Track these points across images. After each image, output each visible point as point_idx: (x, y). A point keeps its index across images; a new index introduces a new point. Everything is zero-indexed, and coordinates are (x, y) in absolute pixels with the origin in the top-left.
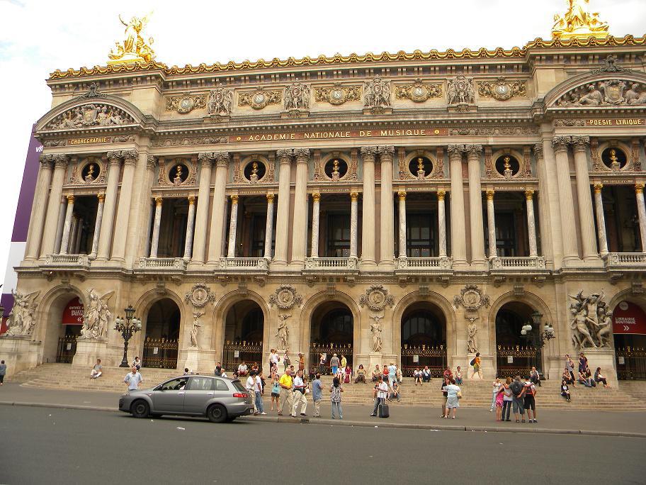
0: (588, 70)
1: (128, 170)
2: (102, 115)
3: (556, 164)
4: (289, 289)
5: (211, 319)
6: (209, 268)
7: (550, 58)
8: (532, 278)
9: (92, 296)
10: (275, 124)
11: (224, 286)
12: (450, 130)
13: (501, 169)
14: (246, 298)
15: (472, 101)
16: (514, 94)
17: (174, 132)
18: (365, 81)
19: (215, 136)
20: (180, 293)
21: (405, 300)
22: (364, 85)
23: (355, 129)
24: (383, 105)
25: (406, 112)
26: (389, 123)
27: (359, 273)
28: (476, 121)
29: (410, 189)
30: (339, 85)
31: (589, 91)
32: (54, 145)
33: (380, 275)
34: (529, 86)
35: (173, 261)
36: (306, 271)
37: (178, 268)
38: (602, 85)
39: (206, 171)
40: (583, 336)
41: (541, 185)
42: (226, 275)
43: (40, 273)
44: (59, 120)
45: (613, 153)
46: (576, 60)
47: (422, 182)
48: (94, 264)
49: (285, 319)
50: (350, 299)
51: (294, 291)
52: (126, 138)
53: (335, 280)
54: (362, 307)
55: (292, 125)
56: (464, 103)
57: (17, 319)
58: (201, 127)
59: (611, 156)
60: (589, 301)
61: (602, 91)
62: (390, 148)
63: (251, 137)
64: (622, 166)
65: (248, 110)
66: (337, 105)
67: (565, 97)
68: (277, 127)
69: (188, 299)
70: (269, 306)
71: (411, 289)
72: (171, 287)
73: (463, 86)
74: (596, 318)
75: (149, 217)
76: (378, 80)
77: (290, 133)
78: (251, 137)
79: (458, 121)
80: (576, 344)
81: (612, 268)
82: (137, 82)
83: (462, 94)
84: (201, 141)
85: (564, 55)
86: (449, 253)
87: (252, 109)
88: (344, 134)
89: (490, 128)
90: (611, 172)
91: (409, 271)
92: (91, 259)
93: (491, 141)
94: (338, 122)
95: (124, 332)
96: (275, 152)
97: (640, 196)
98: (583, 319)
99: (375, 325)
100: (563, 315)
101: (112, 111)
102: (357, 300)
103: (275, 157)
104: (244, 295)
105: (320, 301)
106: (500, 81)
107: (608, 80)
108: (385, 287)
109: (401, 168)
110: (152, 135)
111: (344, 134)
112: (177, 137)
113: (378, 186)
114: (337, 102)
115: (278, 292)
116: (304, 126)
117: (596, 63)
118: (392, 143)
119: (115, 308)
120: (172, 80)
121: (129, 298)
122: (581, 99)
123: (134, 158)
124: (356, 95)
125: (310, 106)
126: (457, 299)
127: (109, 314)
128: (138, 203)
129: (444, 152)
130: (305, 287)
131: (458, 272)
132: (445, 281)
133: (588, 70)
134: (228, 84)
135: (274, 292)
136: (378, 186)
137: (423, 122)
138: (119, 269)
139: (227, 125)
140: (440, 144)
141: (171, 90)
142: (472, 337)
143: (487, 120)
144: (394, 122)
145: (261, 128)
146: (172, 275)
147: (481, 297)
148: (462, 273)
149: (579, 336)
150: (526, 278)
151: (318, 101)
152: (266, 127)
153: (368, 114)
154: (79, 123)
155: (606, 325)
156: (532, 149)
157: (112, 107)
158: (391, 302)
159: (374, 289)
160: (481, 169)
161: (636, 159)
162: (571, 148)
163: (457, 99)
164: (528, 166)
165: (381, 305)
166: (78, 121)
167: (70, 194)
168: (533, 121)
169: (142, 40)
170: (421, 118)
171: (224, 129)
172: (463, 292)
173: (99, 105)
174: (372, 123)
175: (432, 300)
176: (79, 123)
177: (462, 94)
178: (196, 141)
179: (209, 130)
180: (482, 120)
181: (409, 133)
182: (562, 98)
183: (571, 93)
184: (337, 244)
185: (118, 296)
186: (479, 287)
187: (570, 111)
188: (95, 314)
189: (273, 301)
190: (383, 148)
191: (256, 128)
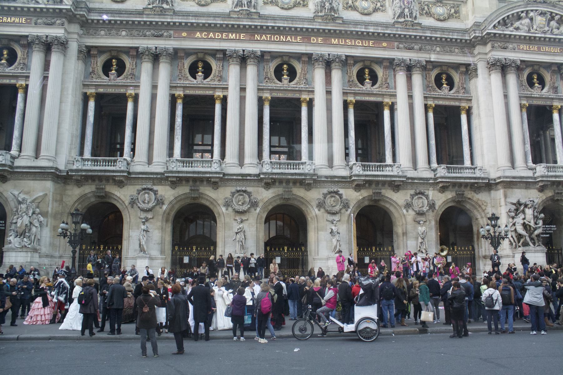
1: (55, 58)
3: (490, 83)
4: (245, 191)
5: (159, 224)
6: (157, 167)
8: (472, 185)
9: (20, 199)
10: (226, 22)
11: (174, 188)
12: (396, 44)
13: (439, 85)
14: (196, 202)
16: (450, 17)
19: (158, 29)
20: (122, 195)
23: (308, 34)
25: (356, 23)
26: (340, 31)
28: (421, 37)
31: (519, 18)
33: (337, 180)
35: (115, 161)
36: (263, 174)
37: (122, 169)
38: (531, 14)
39: (146, 67)
42: (177, 177)
48: (18, 163)
49: (242, 221)
50: (306, 203)
51: (249, 194)
52: (53, 21)
53: (291, 184)
54: (319, 210)
55: (243, 25)
58: (143, 18)
59: (533, 79)
60: (526, 206)
61: (531, 19)
62: (341, 56)
64: (543, 88)
66: (286, 9)
67: (501, 22)
68: (227, 25)
69: (133, 203)
70: (224, 209)
74: (532, 222)
75: (81, 113)
77: (240, 33)
78: (198, 35)
79: (405, 35)
80: (514, 244)
81: (542, 177)
83: (407, 10)
84: (141, 34)
87: (197, 5)
88: (296, 39)
89: (432, 45)
91: (366, 176)
92: (13, 158)
93: (433, 57)
94: (291, 25)
95: (71, 239)
96: (224, 52)
97: (556, 116)
98: (522, 222)
99: (333, 228)
102: (314, 204)
103: (224, 56)
104: (194, 198)
105: (275, 204)
107: (536, 10)
108: (341, 191)
109: (350, 77)
110: (83, 21)
111: (296, 39)
113: (329, 93)
114: (286, 6)
115: (233, 194)
116: (256, 26)
119: (47, 212)
121: (61, 201)
122: (515, 26)
123: (63, 45)
125: (259, 8)
126: (407, 204)
127: (42, 219)
128: (70, 96)
129: (391, 64)
131: (409, 178)
135: (228, 195)
136: (329, 93)
137: (373, 33)
138: (52, 168)
139: (172, 19)
140: (387, 57)
142: (423, 239)
143: (431, 37)
144: (346, 31)
145: (210, 24)
146: (115, 176)
147: (428, 202)
149: (516, 237)
150: (466, 185)
152: (216, 25)
156: (467, 68)
158: (346, 206)
159: (330, 193)
161: (554, 83)
162: (503, 68)
163: (402, 15)
165: (337, 208)
168: (470, 42)
170: (371, 30)
171: (169, 23)
172: (412, 196)
174: (324, 30)
175: (382, 203)
177: (407, 10)
178: (135, 33)
179: (151, 22)
180: (426, 37)
181: (359, 43)
182: (499, 22)
183: (506, 18)
185: (51, 199)
186: (427, 192)
187: (505, 35)
188: (26, 220)
189: (227, 205)
190: (334, 56)
191: (204, 24)
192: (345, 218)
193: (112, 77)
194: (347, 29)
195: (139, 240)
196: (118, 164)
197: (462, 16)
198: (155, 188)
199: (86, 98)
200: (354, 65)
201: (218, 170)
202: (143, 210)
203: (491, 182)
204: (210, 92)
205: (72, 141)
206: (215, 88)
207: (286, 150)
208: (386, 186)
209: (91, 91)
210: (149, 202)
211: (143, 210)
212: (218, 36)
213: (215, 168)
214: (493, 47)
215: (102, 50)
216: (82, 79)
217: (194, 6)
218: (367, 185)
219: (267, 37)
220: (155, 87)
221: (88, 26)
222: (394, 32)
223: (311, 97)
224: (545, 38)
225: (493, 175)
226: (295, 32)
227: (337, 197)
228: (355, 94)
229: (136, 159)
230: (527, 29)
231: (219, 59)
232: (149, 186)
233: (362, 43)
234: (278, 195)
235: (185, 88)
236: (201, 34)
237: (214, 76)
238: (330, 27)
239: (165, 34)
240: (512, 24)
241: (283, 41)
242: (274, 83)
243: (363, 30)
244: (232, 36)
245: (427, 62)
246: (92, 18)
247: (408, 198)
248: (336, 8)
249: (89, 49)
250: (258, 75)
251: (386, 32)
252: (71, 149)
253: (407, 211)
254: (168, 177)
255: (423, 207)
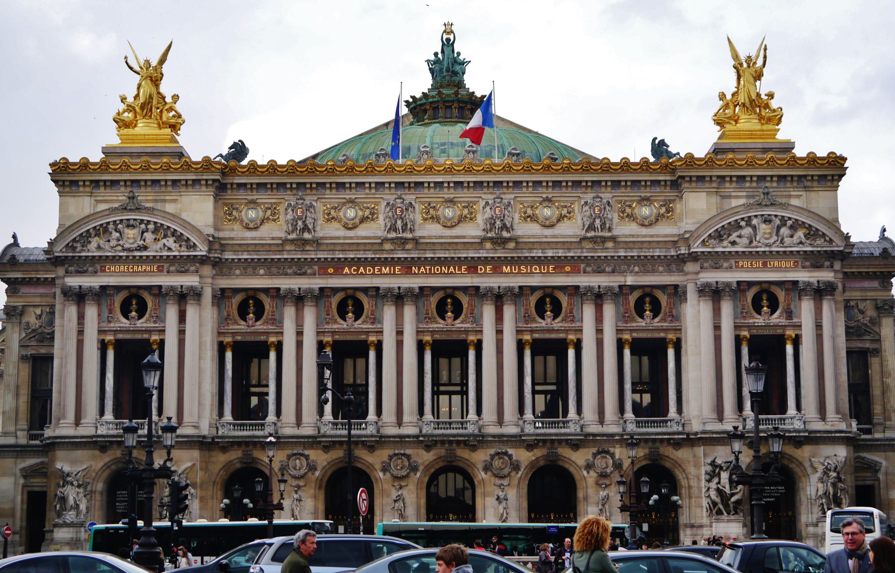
0: (745, 194)
1: (191, 312)
2: (149, 236)
4: (404, 455)
5: (312, 492)
6: (307, 430)
7: (701, 179)
10: (377, 256)
11: (326, 453)
12: (582, 266)
15: (610, 229)
16: (659, 218)
17: (246, 259)
18: (484, 196)
19: (300, 268)
21: (532, 464)
22: (482, 203)
23: (472, 265)
24: (505, 234)
27: (483, 436)
29: (536, 336)
30: (451, 201)
31: (741, 227)
32: (81, 272)
34: (678, 207)
36: (424, 436)
39: (289, 313)
40: (715, 504)
41: (683, 331)
43: (96, 442)
44: (85, 238)
45: (765, 297)
46: (731, 181)
47: (549, 326)
49: (401, 487)
50: (473, 465)
51: (408, 457)
56: (600, 234)
57: (71, 501)
59: (762, 300)
61: (754, 228)
62: (513, 288)
63: (346, 270)
64: (772, 313)
65: (337, 229)
70: (381, 474)
71: (539, 453)
72: (257, 454)
73: (600, 210)
76: (499, 200)
79: (593, 257)
82: (186, 185)
83: (598, 221)
85: (718, 177)
86: (579, 411)
87: (343, 228)
88: (460, 269)
90: (760, 320)
93: (630, 280)
94: (453, 255)
96: (378, 289)
99: (500, 494)
100: (699, 480)
101: (162, 231)
102: (480, 466)
103: (375, 292)
105: (437, 467)
106: (645, 201)
107: (762, 215)
108: (510, 451)
109: (526, 309)
112: (250, 267)
113: (499, 332)
114: (449, 224)
115: (391, 458)
116: (413, 258)
117: (754, 184)
118: (515, 282)
120: (231, 181)
122: (732, 238)
123: (196, 294)
124: (471, 213)
126: (588, 464)
130: (422, 452)
132: (575, 445)
133: (745, 194)
134: (308, 192)
135: (386, 459)
136: (499, 332)
137: (553, 257)
138: (199, 436)
141: (229, 195)
142: (603, 505)
143: (626, 257)
148: (594, 435)
151: (425, 219)
152: (366, 259)
153: (488, 245)
154: (117, 245)
155: (737, 493)
157: (162, 225)
159: (498, 454)
160: (617, 313)
161: (789, 305)
163: (592, 227)
164: (671, 309)
165: (506, 471)
166: (113, 243)
167: (109, 338)
169: (164, 98)
170: (550, 253)
171: (312, 259)
172: (595, 455)
173: (142, 220)
175: (561, 463)
176: (117, 245)
177: (598, 221)
178: (274, 270)
180: (619, 257)
181: (536, 269)
184: (442, 388)
186: (612, 450)
189: (385, 470)
190: (505, 288)
192: (515, 482)
193: (251, 323)
194: (520, 255)
195: (293, 510)
196: (266, 428)
197: (676, 216)
198: (307, 452)
199: (221, 349)
200: (532, 294)
201: (374, 432)
202: (295, 477)
203: (692, 437)
204: (363, 337)
205: (212, 400)
206: (368, 332)
207: (458, 388)
208: (564, 444)
209: (228, 339)
210: (300, 469)
211: (295, 477)
212: (370, 270)
213: (371, 430)
214: (702, 268)
215: (236, 291)
216: (216, 326)
217: (339, 229)
218: (541, 444)
219: (426, 269)
220: (300, 333)
221: (220, 266)
222: (579, 255)
223: (479, 337)
224: (771, 252)
225: (696, 427)
226: (459, 262)
227: (506, 458)
228: (532, 331)
229: (283, 417)
230: (745, 241)
231: (372, 296)
232: (300, 451)
233: (540, 269)
234: (441, 457)
235: (333, 333)
236: (350, 269)
237: (367, 317)
238: (500, 254)
239: (309, 271)
240: (729, 235)
241: (445, 273)
242: (437, 323)
243: (540, 255)
244: (385, 270)
245: (620, 287)
246: (226, 257)
247: (590, 458)
248: (508, 225)
249: (223, 290)
250: (417, 314)
251: (568, 255)
252: (212, 410)
253: (588, 473)
254: (321, 442)
255: (607, 467)
